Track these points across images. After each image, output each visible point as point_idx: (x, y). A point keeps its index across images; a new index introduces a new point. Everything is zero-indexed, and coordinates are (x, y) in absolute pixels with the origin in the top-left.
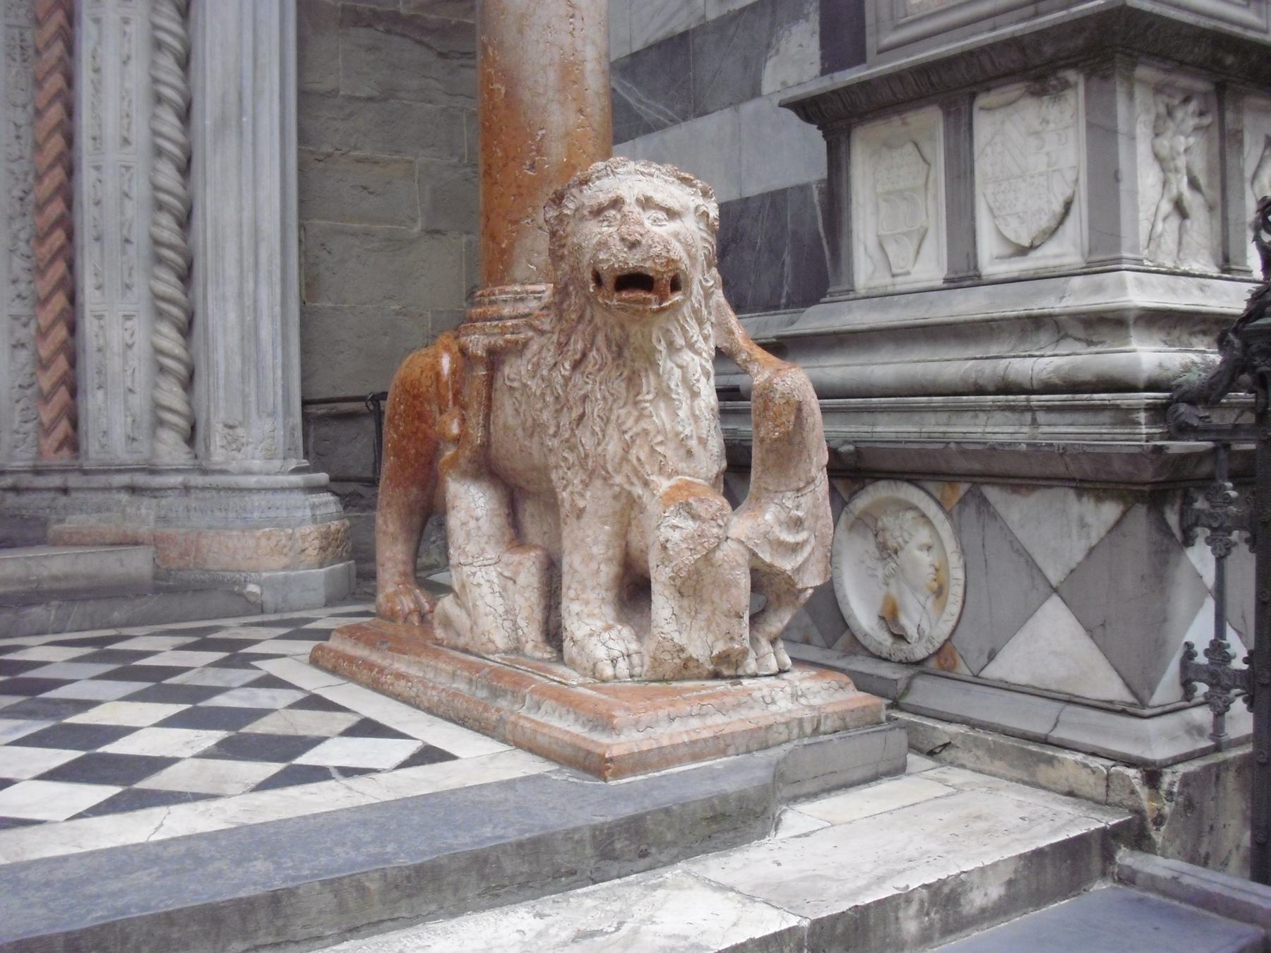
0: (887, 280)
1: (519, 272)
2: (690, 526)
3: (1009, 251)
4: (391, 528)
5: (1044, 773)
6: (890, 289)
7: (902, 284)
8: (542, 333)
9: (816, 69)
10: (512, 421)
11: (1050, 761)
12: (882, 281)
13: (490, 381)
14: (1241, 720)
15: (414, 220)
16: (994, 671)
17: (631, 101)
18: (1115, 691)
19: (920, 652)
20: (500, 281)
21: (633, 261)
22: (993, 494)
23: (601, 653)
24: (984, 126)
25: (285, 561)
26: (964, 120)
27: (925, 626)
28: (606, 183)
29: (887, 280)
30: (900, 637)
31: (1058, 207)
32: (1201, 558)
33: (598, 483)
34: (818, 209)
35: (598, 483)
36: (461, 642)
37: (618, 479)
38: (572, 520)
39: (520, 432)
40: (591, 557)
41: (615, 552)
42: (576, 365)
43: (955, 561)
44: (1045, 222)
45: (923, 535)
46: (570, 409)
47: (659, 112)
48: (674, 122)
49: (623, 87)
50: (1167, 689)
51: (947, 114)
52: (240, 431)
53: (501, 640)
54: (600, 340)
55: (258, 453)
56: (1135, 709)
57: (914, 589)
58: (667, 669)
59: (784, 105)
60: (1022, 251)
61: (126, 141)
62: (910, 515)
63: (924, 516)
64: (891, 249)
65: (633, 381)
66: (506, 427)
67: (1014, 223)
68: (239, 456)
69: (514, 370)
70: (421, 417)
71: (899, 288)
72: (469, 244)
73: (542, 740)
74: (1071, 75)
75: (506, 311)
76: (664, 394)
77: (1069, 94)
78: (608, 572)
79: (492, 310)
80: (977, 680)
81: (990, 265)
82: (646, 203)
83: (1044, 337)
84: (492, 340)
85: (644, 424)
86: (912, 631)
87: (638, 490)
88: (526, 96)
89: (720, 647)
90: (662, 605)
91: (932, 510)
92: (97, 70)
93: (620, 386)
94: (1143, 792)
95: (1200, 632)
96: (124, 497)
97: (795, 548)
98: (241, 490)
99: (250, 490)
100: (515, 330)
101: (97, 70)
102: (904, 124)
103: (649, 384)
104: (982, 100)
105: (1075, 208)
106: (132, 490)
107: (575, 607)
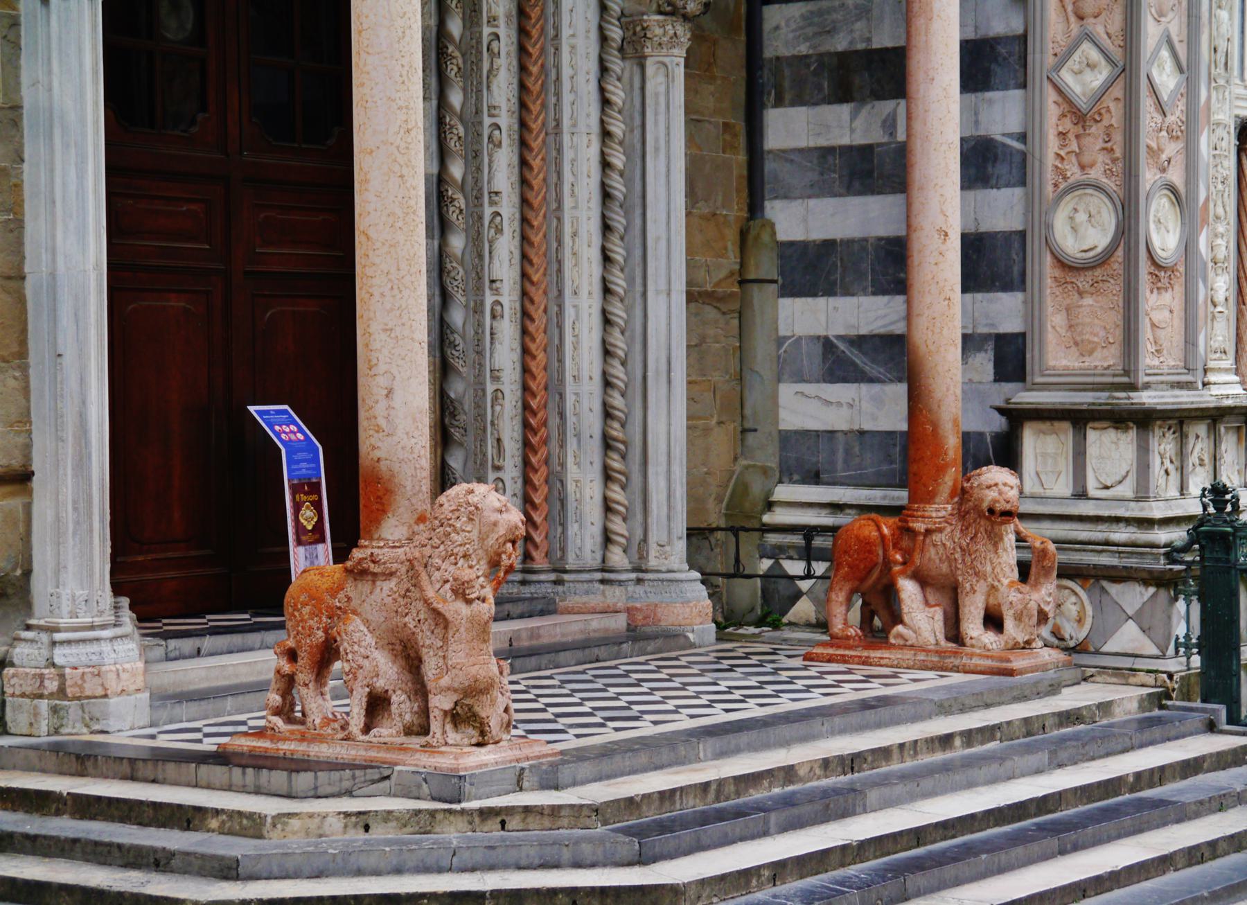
0: (1041, 490)
1: (937, 500)
2: (1020, 596)
3: (1101, 486)
4: (841, 599)
5: (1132, 680)
6: (1043, 495)
7: (1049, 493)
8: (951, 525)
9: (991, 377)
10: (933, 556)
11: (1134, 675)
12: (1038, 490)
13: (924, 541)
14: (1196, 661)
15: (712, 416)
16: (1105, 649)
17: (858, 361)
18: (1155, 651)
19: (1072, 644)
20: (929, 503)
21: (1008, 507)
22: (1105, 583)
23: (987, 641)
24: (1092, 435)
25: (701, 620)
26: (1083, 431)
27: (1073, 634)
28: (989, 475)
29: (1041, 490)
30: (1062, 639)
31: (1124, 473)
32: (1181, 605)
33: (982, 581)
34: (990, 446)
35: (982, 581)
36: (909, 643)
37: (990, 580)
38: (971, 595)
39: (937, 561)
40: (977, 607)
41: (984, 606)
42: (972, 539)
43: (1089, 610)
44: (1118, 478)
45: (1073, 599)
46: (970, 555)
47: (880, 373)
48: (891, 381)
49: (851, 352)
50: (1171, 650)
51: (1074, 427)
52: (667, 548)
53: (933, 641)
54: (982, 529)
55: (677, 561)
56: (1163, 656)
57: (1068, 620)
58: (1009, 646)
59: (991, 407)
60: (1107, 488)
61: (591, 378)
62: (1067, 591)
63: (1073, 591)
64: (1043, 477)
65: (996, 545)
66: (930, 559)
67: (1104, 475)
68: (666, 562)
69: (936, 537)
70: (870, 552)
71: (1047, 495)
72: (735, 428)
73: (979, 668)
74: (1131, 424)
75: (934, 515)
76: (1005, 550)
77: (1130, 431)
78: (982, 613)
79: (927, 514)
80: (1097, 652)
81: (1092, 492)
82: (1005, 484)
83: (1121, 525)
84: (929, 526)
85: (999, 560)
86: (1067, 636)
87: (996, 583)
88: (941, 432)
89: (1026, 638)
90: (1009, 624)
91: (1078, 589)
92: (576, 336)
93: (990, 547)
94: (1168, 681)
95: (1180, 630)
96: (597, 585)
97: (1049, 603)
98: (677, 581)
99: (682, 581)
100: (940, 523)
101: (576, 336)
102: (1052, 425)
103: (1000, 546)
104: (1090, 425)
105: (1130, 474)
106: (602, 581)
107: (971, 626)
